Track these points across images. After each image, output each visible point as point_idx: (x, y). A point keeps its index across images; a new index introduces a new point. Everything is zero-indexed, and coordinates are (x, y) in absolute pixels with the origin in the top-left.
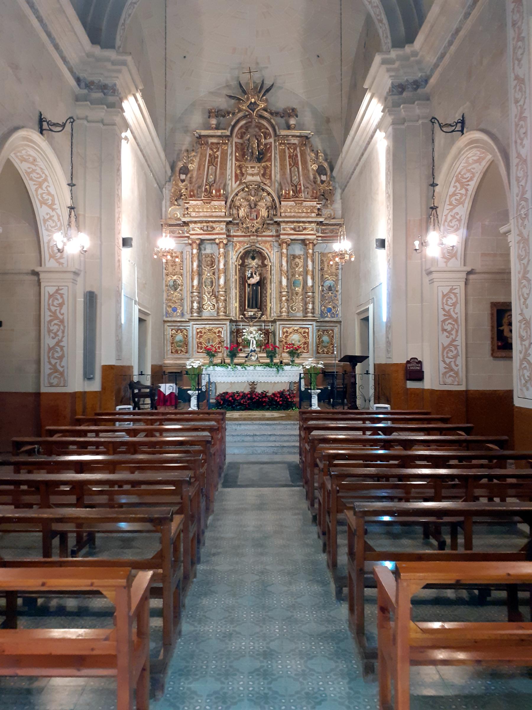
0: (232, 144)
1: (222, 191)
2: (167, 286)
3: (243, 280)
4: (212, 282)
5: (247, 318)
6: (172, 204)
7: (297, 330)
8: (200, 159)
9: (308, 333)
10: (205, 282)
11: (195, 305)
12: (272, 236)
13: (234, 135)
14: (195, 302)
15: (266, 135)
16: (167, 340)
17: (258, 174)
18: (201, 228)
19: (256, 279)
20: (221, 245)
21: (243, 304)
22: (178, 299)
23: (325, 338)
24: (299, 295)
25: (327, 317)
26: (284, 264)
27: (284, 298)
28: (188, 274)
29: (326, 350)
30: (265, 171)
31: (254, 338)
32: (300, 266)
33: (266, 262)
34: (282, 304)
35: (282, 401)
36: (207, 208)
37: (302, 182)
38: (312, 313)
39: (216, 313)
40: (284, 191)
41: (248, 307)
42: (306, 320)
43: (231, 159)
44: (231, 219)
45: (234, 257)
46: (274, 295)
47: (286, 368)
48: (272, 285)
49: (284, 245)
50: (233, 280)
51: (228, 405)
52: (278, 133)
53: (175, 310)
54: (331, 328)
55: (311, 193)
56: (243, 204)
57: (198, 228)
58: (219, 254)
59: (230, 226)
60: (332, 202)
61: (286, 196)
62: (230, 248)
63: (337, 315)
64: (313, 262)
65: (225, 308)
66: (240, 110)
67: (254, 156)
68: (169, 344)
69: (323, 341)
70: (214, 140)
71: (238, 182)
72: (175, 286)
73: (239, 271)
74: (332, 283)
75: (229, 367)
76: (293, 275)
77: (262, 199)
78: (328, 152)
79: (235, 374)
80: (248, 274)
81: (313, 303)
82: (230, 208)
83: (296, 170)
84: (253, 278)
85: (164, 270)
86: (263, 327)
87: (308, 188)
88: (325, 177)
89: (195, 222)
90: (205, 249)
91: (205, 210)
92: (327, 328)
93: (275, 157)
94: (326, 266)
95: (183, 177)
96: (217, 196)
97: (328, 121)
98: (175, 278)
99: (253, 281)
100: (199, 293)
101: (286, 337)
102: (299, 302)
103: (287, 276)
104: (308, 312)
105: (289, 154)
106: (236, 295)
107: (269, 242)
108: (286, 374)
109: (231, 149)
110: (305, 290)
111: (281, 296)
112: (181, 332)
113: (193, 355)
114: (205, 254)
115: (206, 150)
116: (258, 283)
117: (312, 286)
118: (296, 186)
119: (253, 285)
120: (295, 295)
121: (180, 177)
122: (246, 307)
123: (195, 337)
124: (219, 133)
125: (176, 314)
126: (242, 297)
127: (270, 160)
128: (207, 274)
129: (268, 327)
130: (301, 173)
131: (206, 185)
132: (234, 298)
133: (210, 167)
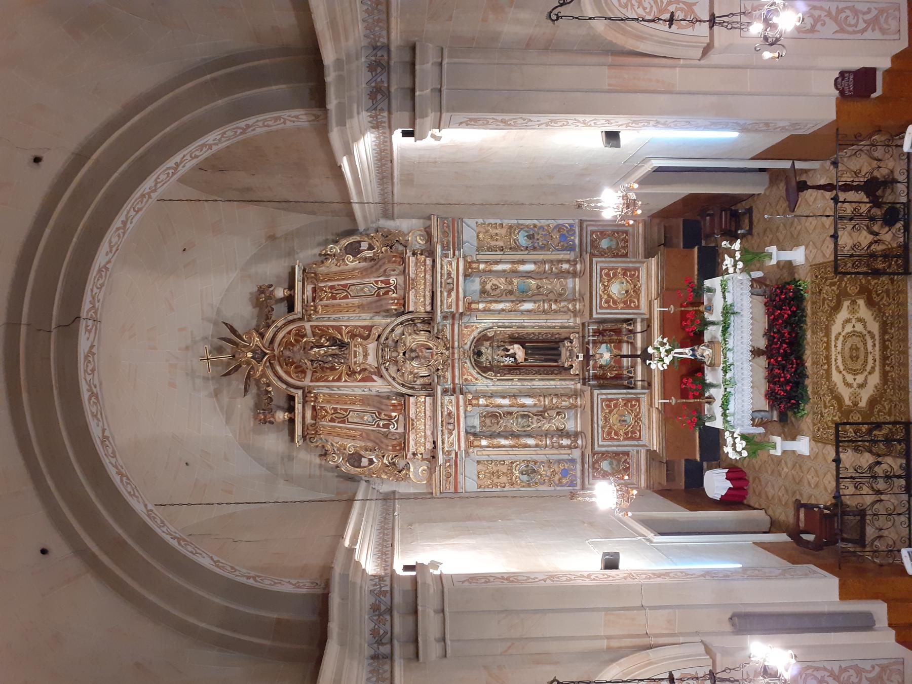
2: (529, 485)
3: (515, 369)
4: (523, 416)
10: (523, 427)
14: (561, 442)
15: (300, 334)
22: (549, 467)
23: (604, 244)
25: (573, 241)
26: (501, 306)
27: (554, 307)
28: (511, 452)
32: (495, 282)
33: (490, 335)
41: (556, 361)
43: (338, 387)
45: (483, 383)
46: (542, 322)
48: (526, 324)
50: (519, 384)
52: (300, 316)
54: (589, 236)
56: (409, 370)
57: (448, 438)
61: (400, 304)
64: (497, 262)
66: (264, 375)
67: (337, 352)
69: (609, 248)
71: (374, 377)
72: (530, 471)
78: (321, 238)
82: (413, 388)
85: (505, 489)
87: (385, 271)
88: (362, 244)
90: (474, 427)
92: (589, 240)
93: (334, 320)
94: (497, 243)
95: (365, 462)
98: (517, 473)
101: (615, 302)
103: (520, 302)
105: (328, 299)
106: (542, 380)
108: (739, 300)
109: (322, 389)
113: (644, 446)
114: (482, 426)
117: (535, 263)
118: (379, 288)
119: (526, 354)
120: (541, 290)
121: (365, 467)
128: (514, 425)
129: (591, 331)
130: (359, 281)
132: (547, 383)
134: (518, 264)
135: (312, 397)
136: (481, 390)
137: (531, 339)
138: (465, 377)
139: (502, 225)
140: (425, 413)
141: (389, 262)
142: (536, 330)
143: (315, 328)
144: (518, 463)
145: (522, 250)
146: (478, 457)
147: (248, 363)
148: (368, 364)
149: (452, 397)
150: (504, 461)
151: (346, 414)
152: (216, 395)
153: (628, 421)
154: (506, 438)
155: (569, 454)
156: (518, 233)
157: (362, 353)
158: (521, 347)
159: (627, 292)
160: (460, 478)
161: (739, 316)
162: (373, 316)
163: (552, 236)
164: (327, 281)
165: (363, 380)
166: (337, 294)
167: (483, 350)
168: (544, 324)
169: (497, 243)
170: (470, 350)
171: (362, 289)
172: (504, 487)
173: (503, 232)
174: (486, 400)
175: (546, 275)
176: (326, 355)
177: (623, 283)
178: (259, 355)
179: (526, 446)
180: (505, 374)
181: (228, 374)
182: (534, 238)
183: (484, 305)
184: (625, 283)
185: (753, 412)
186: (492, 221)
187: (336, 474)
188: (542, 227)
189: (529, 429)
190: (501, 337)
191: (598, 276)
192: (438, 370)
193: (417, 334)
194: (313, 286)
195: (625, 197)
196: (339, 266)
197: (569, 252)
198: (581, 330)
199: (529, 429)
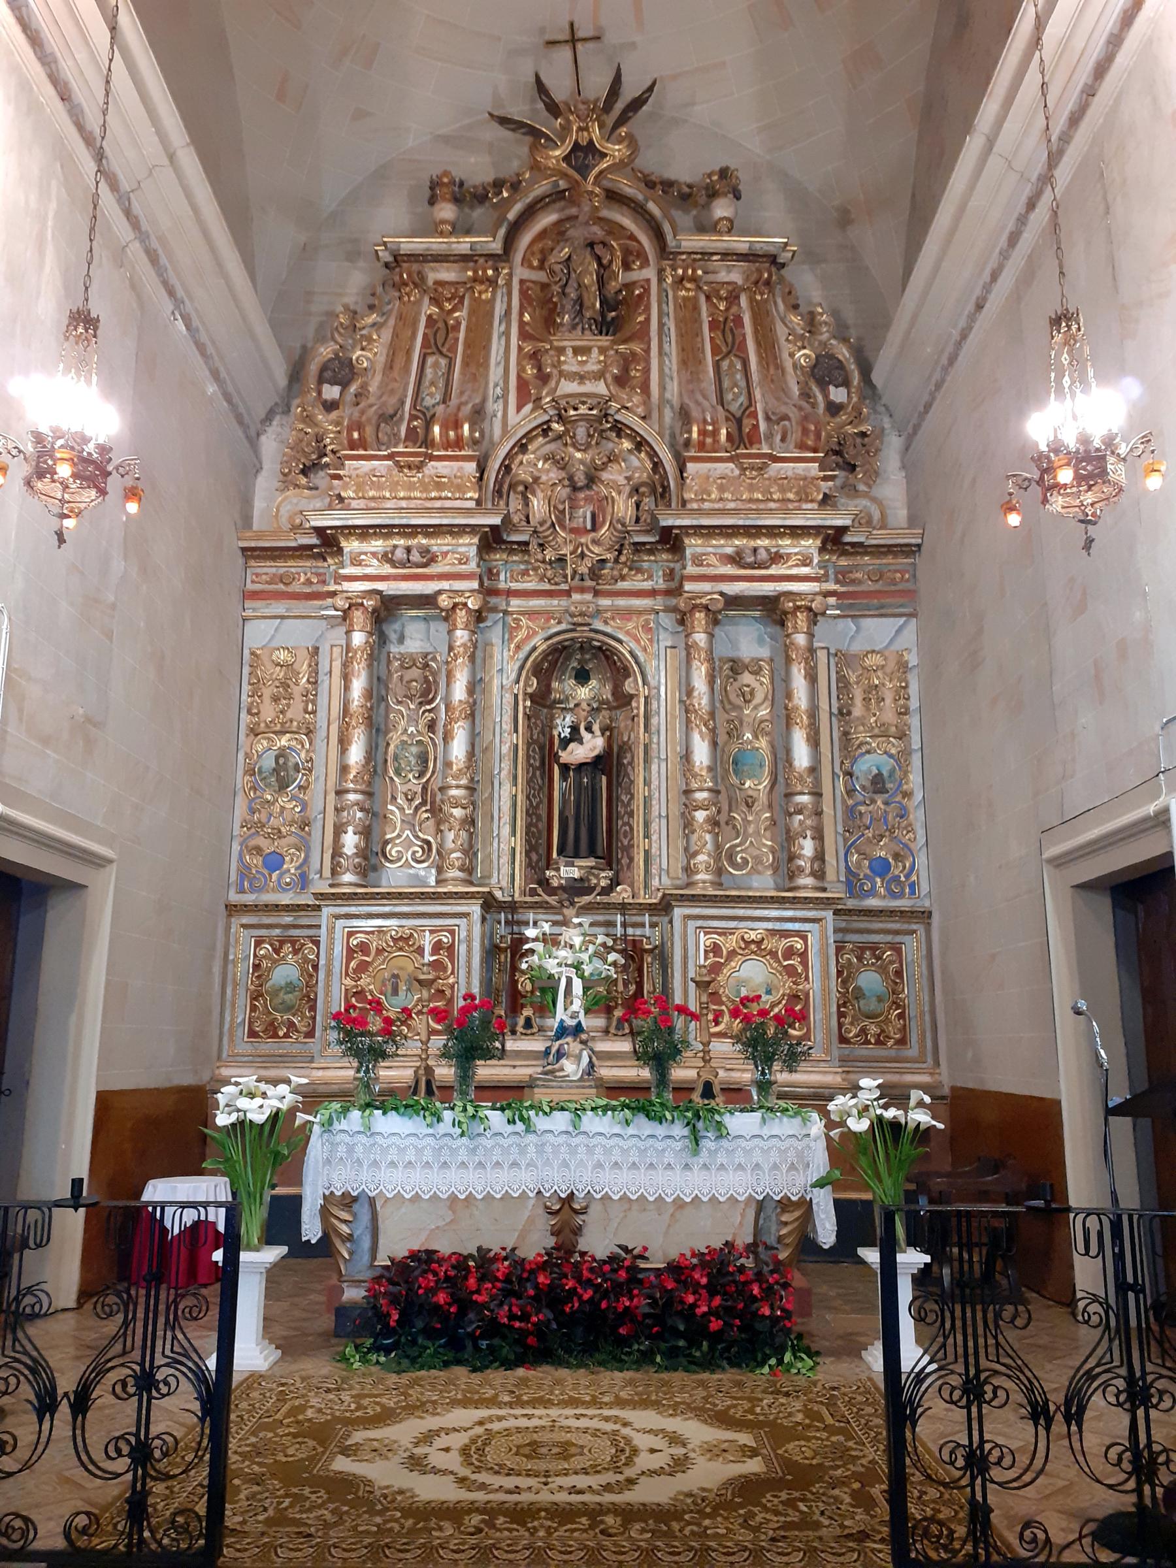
0: (509, 284)
1: (466, 427)
2: (251, 772)
4: (423, 759)
5: (552, 891)
6: (286, 482)
7: (759, 943)
8: (395, 335)
9: (804, 955)
10: (396, 758)
11: (351, 841)
12: (652, 593)
13: (518, 257)
14: (350, 829)
16: (235, 985)
17: (599, 375)
18: (385, 555)
19: (590, 746)
20: (461, 616)
21: (543, 841)
23: (869, 980)
24: (757, 807)
25: (872, 893)
26: (700, 684)
27: (700, 816)
29: (874, 1029)
30: (626, 369)
31: (577, 967)
32: (759, 697)
33: (628, 686)
34: (694, 837)
35: (728, 1312)
36: (411, 487)
37: (759, 407)
38: (813, 874)
39: (433, 871)
40: (695, 429)
42: (795, 901)
43: (507, 334)
44: (496, 520)
47: (741, 1123)
48: (654, 767)
49: (700, 616)
51: (430, 1333)
53: (274, 862)
54: (889, 938)
55: (795, 436)
56: (544, 478)
57: (374, 554)
58: (451, 649)
59: (498, 556)
60: (873, 475)
62: (496, 636)
63: (912, 886)
64: (812, 678)
65: (470, 851)
67: (588, 314)
68: (243, 1000)
69: (859, 994)
70: (447, 274)
73: (528, 717)
74: (887, 763)
75: (447, 1115)
76: (734, 733)
77: (611, 459)
78: (849, 314)
79: (473, 1151)
80: (562, 727)
81: (819, 837)
82: (498, 492)
83: (739, 367)
84: (580, 741)
85: (244, 715)
86: (619, 931)
89: (364, 532)
90: (401, 640)
91: (402, 494)
93: (661, 325)
94: (858, 701)
95: (331, 392)
96: (447, 445)
97: (845, 219)
99: (579, 753)
100: (369, 794)
102: (757, 833)
103: (713, 731)
104: (801, 870)
106: (514, 805)
107: (640, 613)
108: (739, 1157)
110: (781, 788)
111: (689, 807)
112: (296, 952)
114: (402, 658)
115: (418, 302)
116: (600, 763)
117: (814, 770)
118: (739, 422)
119: (581, 766)
121: (320, 393)
122: (555, 855)
123: (337, 966)
124: (463, 244)
125: (280, 877)
126: (539, 818)
127: (642, 334)
129: (638, 932)
130: (755, 377)
131: (413, 418)
132: (506, 818)
133: (430, 360)
135: (485, 271)
136: (491, 657)
137: (618, 798)
139: (905, 714)
142: (640, 790)
143: (642, 287)
144: (307, 746)
145: (842, 763)
146: (328, 647)
150: (314, 712)
151: (444, 350)
153: (394, 1000)
154: (369, 694)
155: (321, 872)
156: (885, 753)
160: (279, 608)
162: (672, 407)
163: (882, 836)
165: (522, 385)
166: (723, 332)
167: (593, 683)
168: (655, 813)
169: (858, 701)
171: (736, 385)
172: (249, 712)
174: (464, 645)
175: (780, 817)
178: (583, 154)
179: (344, 743)
180: (529, 718)
182: (875, 792)
183: (702, 644)
186: (914, 689)
187: (309, 345)
188: (903, 814)
190: (622, 725)
193: (630, 496)
196: (787, 340)
197: (843, 879)
198: (641, 901)
199: (392, 774)
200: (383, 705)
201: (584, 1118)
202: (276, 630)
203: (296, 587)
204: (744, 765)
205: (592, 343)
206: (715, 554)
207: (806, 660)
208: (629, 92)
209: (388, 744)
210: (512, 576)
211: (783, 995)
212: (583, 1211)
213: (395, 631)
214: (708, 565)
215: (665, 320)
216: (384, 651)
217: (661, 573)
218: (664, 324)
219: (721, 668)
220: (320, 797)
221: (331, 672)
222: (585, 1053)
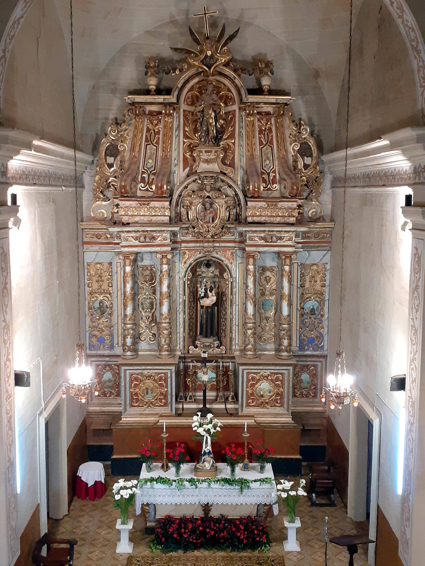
0: (178, 113)
4: (152, 304)
7: (267, 377)
10: (142, 304)
14: (129, 337)
15: (227, 100)
22: (107, 326)
26: (251, 285)
27: (249, 332)
28: (119, 293)
33: (225, 275)
43: (178, 136)
46: (235, 321)
48: (234, 307)
50: (181, 300)
52: (244, 100)
56: (194, 201)
57: (132, 237)
61: (254, 194)
64: (290, 281)
67: (211, 135)
71: (187, 169)
82: (177, 205)
87: (285, 180)
88: (310, 159)
90: (142, 260)
93: (240, 132)
95: (110, 160)
98: (101, 298)
100: (134, 324)
101: (253, 385)
103: (254, 302)
105: (260, 127)
106: (184, 322)
110: (278, 314)
117: (289, 316)
118: (269, 174)
119: (207, 307)
120: (265, 321)
121: (106, 160)
129: (228, 364)
130: (276, 156)
132: (182, 326)
134: (288, 300)
135: (170, 111)
136: (175, 267)
137: (221, 311)
138: (187, 253)
140: (155, 216)
141: (293, 184)
142: (228, 316)
143: (233, 114)
144: (110, 299)
146: (115, 263)
147: (201, 52)
148: (199, 163)
149: (169, 240)
150: (112, 286)
151: (154, 143)
152: (172, 22)
153: (147, 396)
154: (132, 288)
157: (210, 158)
158: (213, 302)
159: (262, 396)
160: (96, 247)
161: (239, 493)
162: (243, 169)
164: (276, 125)
165: (185, 158)
166: (264, 135)
167: (212, 269)
168: (234, 323)
170: (212, 257)
171: (268, 158)
173: (318, 287)
174: (166, 271)
176: (208, 124)
177: (270, 392)
179: (125, 306)
180: (189, 288)
181: (192, 33)
183: (252, 270)
184: (270, 394)
185: (154, 505)
187: (99, 134)
189: (141, 309)
190: (223, 285)
191: (277, 371)
192: (194, 228)
193: (226, 209)
194: (272, 112)
195: (346, 395)
196: (289, 137)
198: (229, 355)
199: (141, 309)
200: (137, 284)
201: (211, 485)
202: (96, 256)
203: (102, 240)
204: (266, 305)
205: (212, 149)
206: (257, 236)
207: (289, 276)
208: (228, 33)
209: (139, 299)
210: (182, 235)
211: (275, 393)
212: (211, 506)
213: (140, 257)
214: (255, 240)
215: (241, 130)
216: (136, 264)
217: (238, 234)
218: (241, 132)
219: (259, 270)
220: (117, 319)
221: (117, 272)
222: (211, 460)
